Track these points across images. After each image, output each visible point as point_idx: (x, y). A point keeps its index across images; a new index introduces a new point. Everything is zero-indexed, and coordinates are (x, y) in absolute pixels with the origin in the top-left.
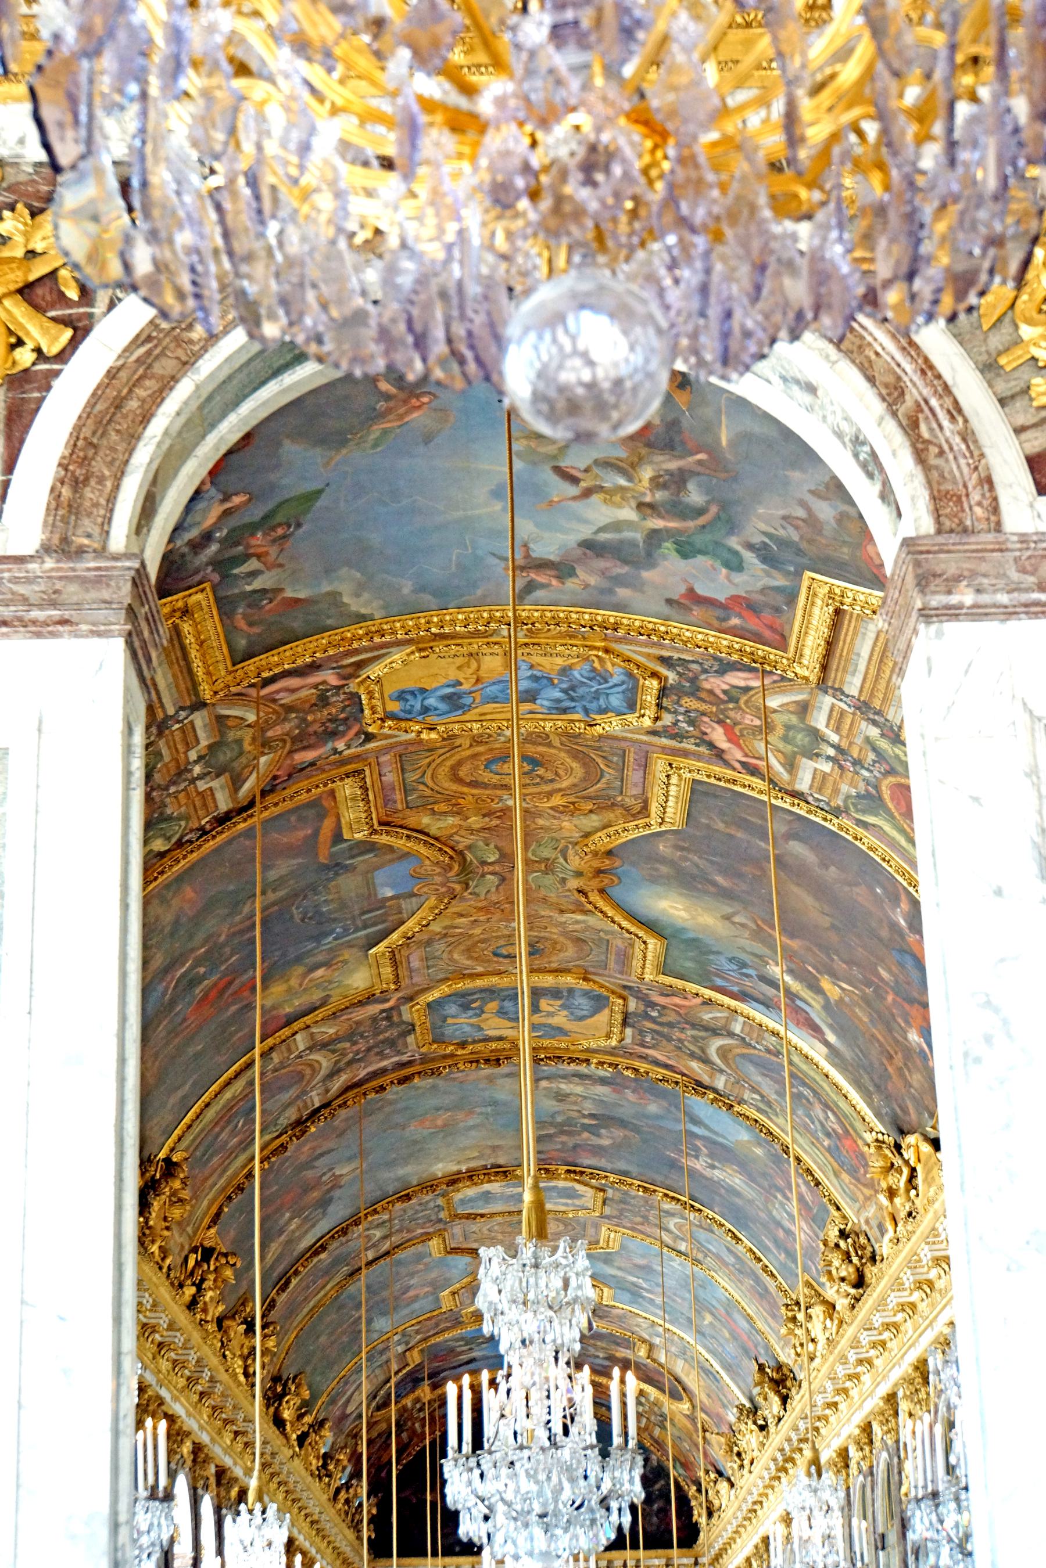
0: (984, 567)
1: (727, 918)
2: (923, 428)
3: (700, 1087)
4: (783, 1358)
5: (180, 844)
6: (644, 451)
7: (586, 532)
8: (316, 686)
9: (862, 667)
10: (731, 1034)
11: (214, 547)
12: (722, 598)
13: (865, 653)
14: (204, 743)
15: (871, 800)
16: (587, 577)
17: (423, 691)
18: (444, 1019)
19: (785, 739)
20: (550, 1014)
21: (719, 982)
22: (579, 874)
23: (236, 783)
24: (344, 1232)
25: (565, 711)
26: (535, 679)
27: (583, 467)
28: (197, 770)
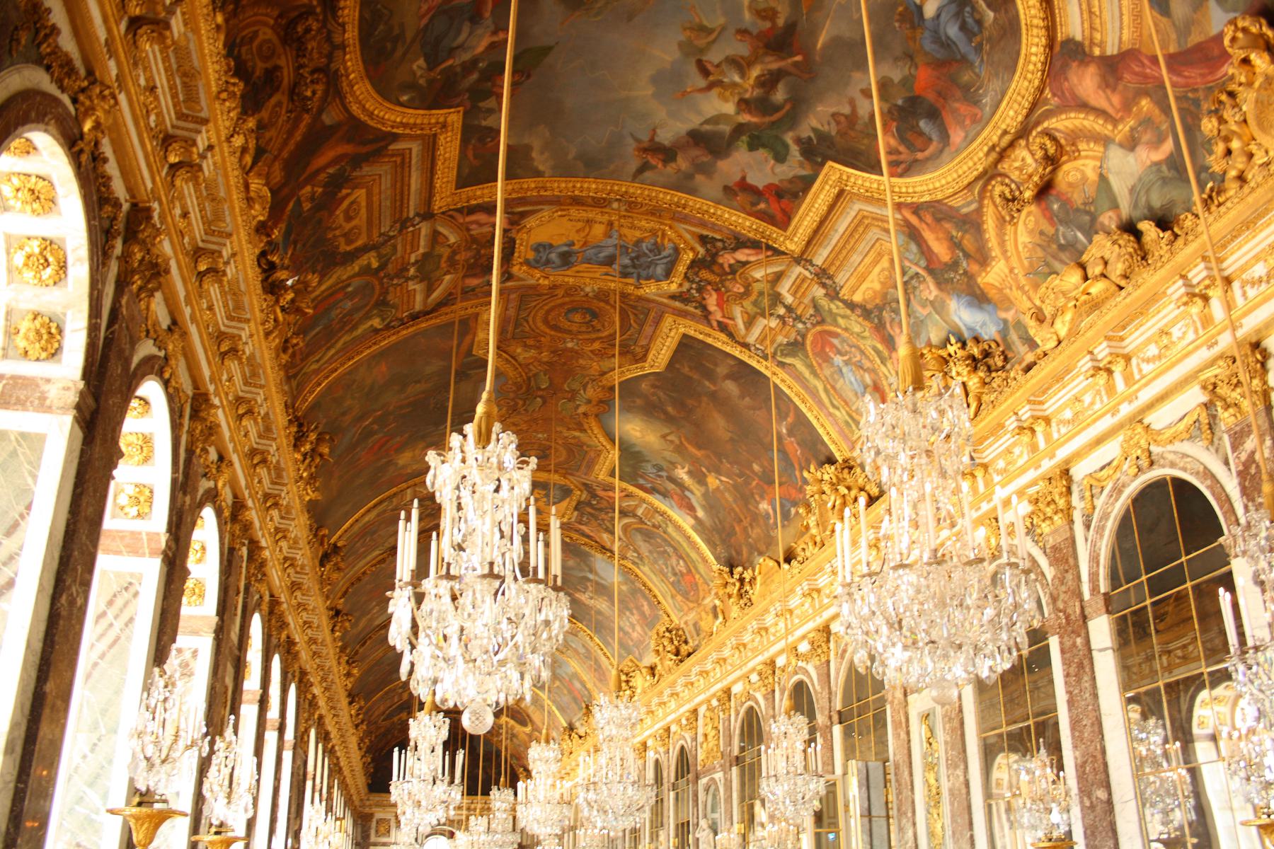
1: (664, 437)
5: (388, 327)
6: (761, 51)
10: (635, 516)
12: (760, 186)
14: (421, 250)
15: (796, 347)
17: (551, 246)
19: (755, 303)
21: (641, 481)
22: (589, 401)
23: (429, 290)
27: (716, 61)
28: (412, 271)
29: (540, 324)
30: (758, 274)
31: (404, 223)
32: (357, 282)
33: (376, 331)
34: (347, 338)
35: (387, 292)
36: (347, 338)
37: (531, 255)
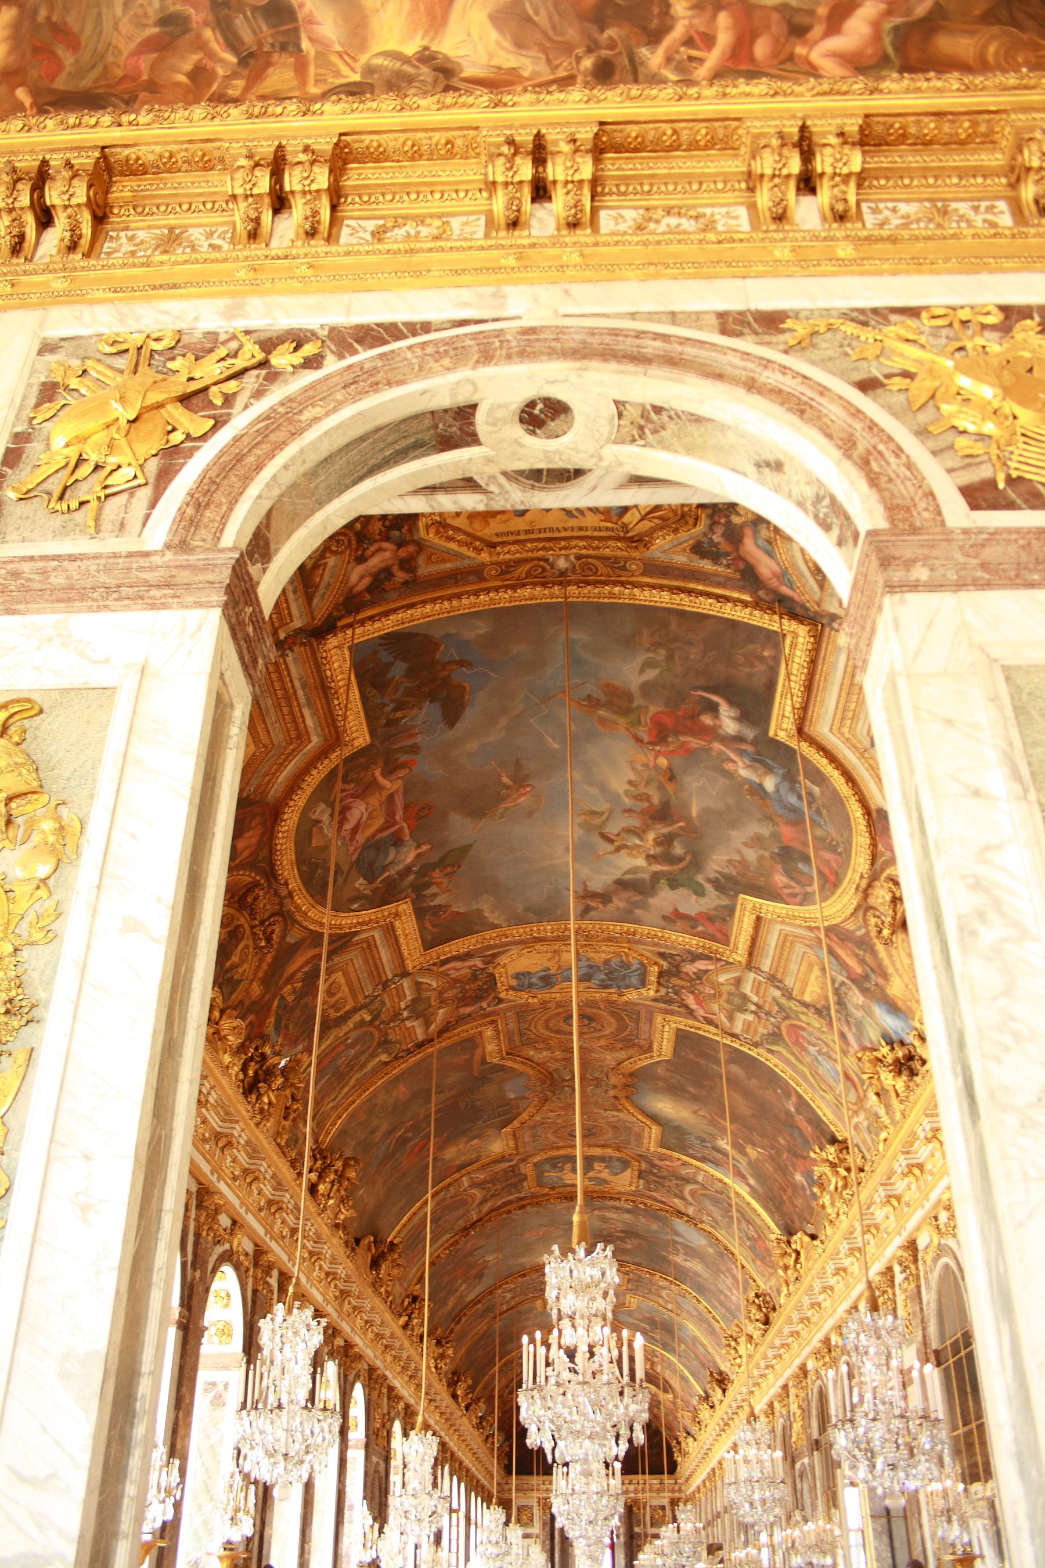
0: (935, 553)
1: (695, 1112)
2: (874, 466)
3: (680, 1214)
4: (723, 1368)
5: (396, 1058)
6: (649, 822)
7: (617, 874)
8: (470, 967)
9: (771, 953)
10: (697, 1182)
11: (412, 877)
12: (693, 914)
13: (773, 944)
14: (409, 998)
15: (775, 1037)
16: (619, 902)
17: (529, 973)
18: (543, 1172)
19: (728, 1001)
20: (600, 1172)
21: (691, 1152)
22: (615, 1087)
23: (427, 1024)
24: (491, 1293)
25: (606, 987)
26: (590, 967)
27: (616, 832)
28: (405, 1014)
29: (543, 1031)
30: (722, 979)
31: (386, 985)
32: (354, 1035)
33: (386, 1064)
34: (358, 1075)
35: (386, 1034)
36: (358, 1075)
37: (514, 982)
